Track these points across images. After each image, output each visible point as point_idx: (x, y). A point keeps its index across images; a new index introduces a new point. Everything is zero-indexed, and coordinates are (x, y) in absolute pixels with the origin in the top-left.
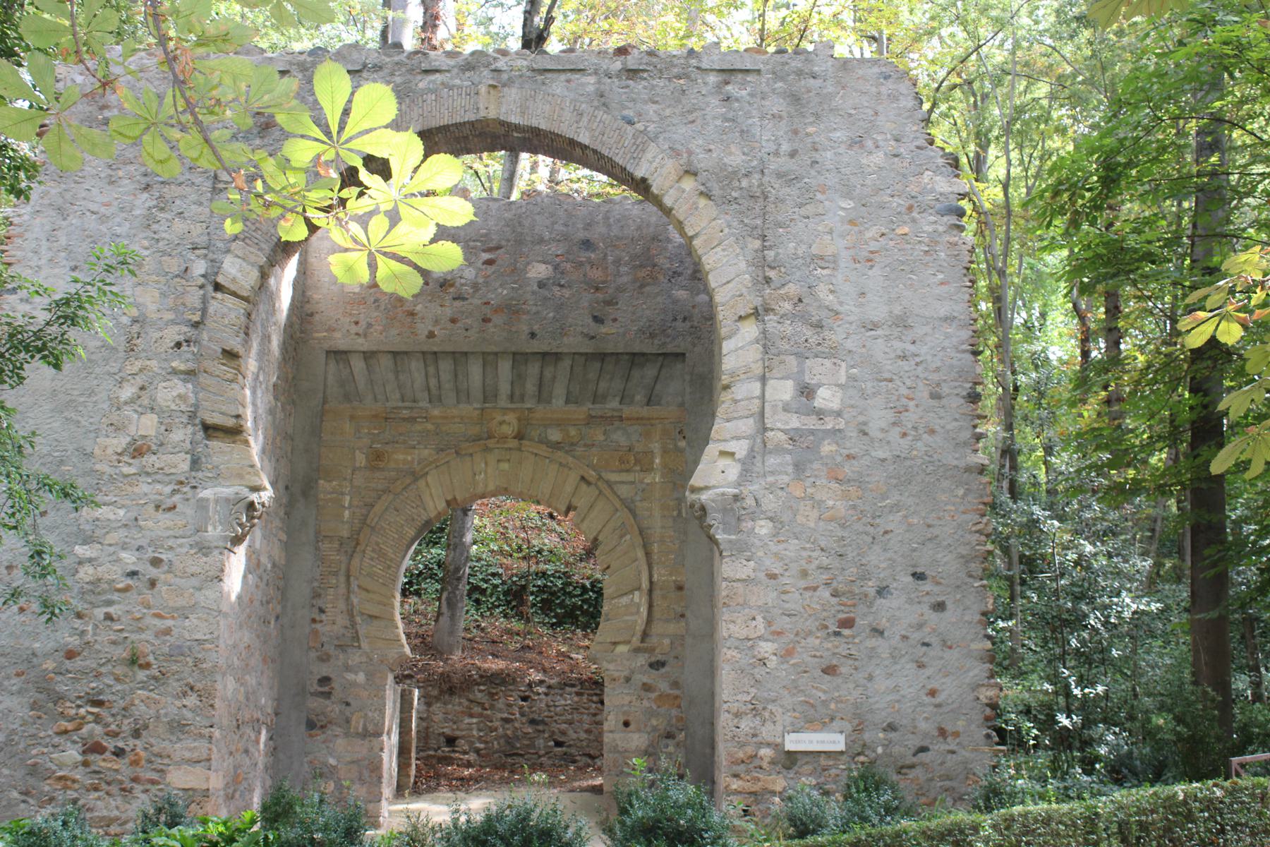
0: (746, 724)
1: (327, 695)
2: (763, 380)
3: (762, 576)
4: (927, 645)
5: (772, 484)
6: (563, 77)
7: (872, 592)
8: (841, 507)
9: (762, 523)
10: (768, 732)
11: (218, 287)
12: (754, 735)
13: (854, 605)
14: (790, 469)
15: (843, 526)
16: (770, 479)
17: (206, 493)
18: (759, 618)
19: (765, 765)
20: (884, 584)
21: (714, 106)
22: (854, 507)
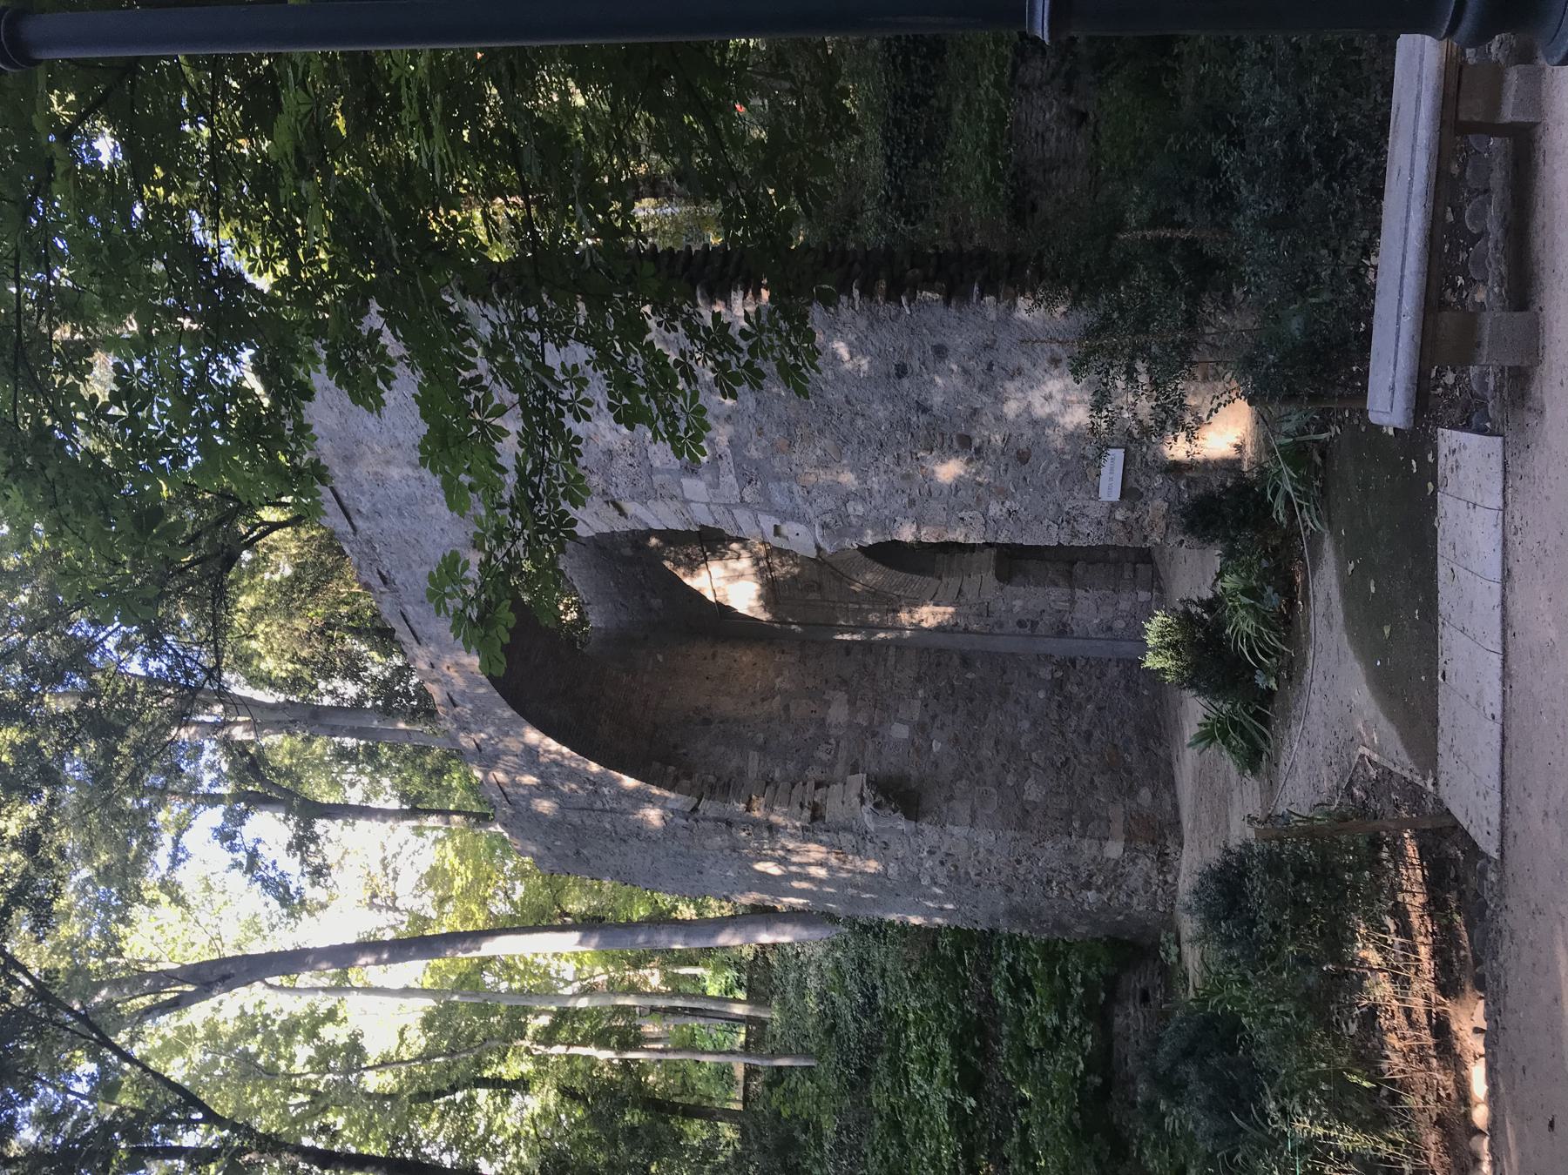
0: (1084, 527)
1: (1034, 624)
2: (686, 502)
3: (910, 512)
4: (990, 365)
5: (806, 500)
6: (416, 627)
7: (924, 419)
8: (827, 442)
9: (850, 510)
10: (1095, 511)
11: (695, 809)
12: (1099, 523)
13: (942, 435)
14: (784, 484)
15: (846, 442)
16: (799, 500)
17: (871, 827)
18: (962, 514)
19: (1136, 515)
20: (914, 405)
21: (390, 523)
22: (821, 432)
